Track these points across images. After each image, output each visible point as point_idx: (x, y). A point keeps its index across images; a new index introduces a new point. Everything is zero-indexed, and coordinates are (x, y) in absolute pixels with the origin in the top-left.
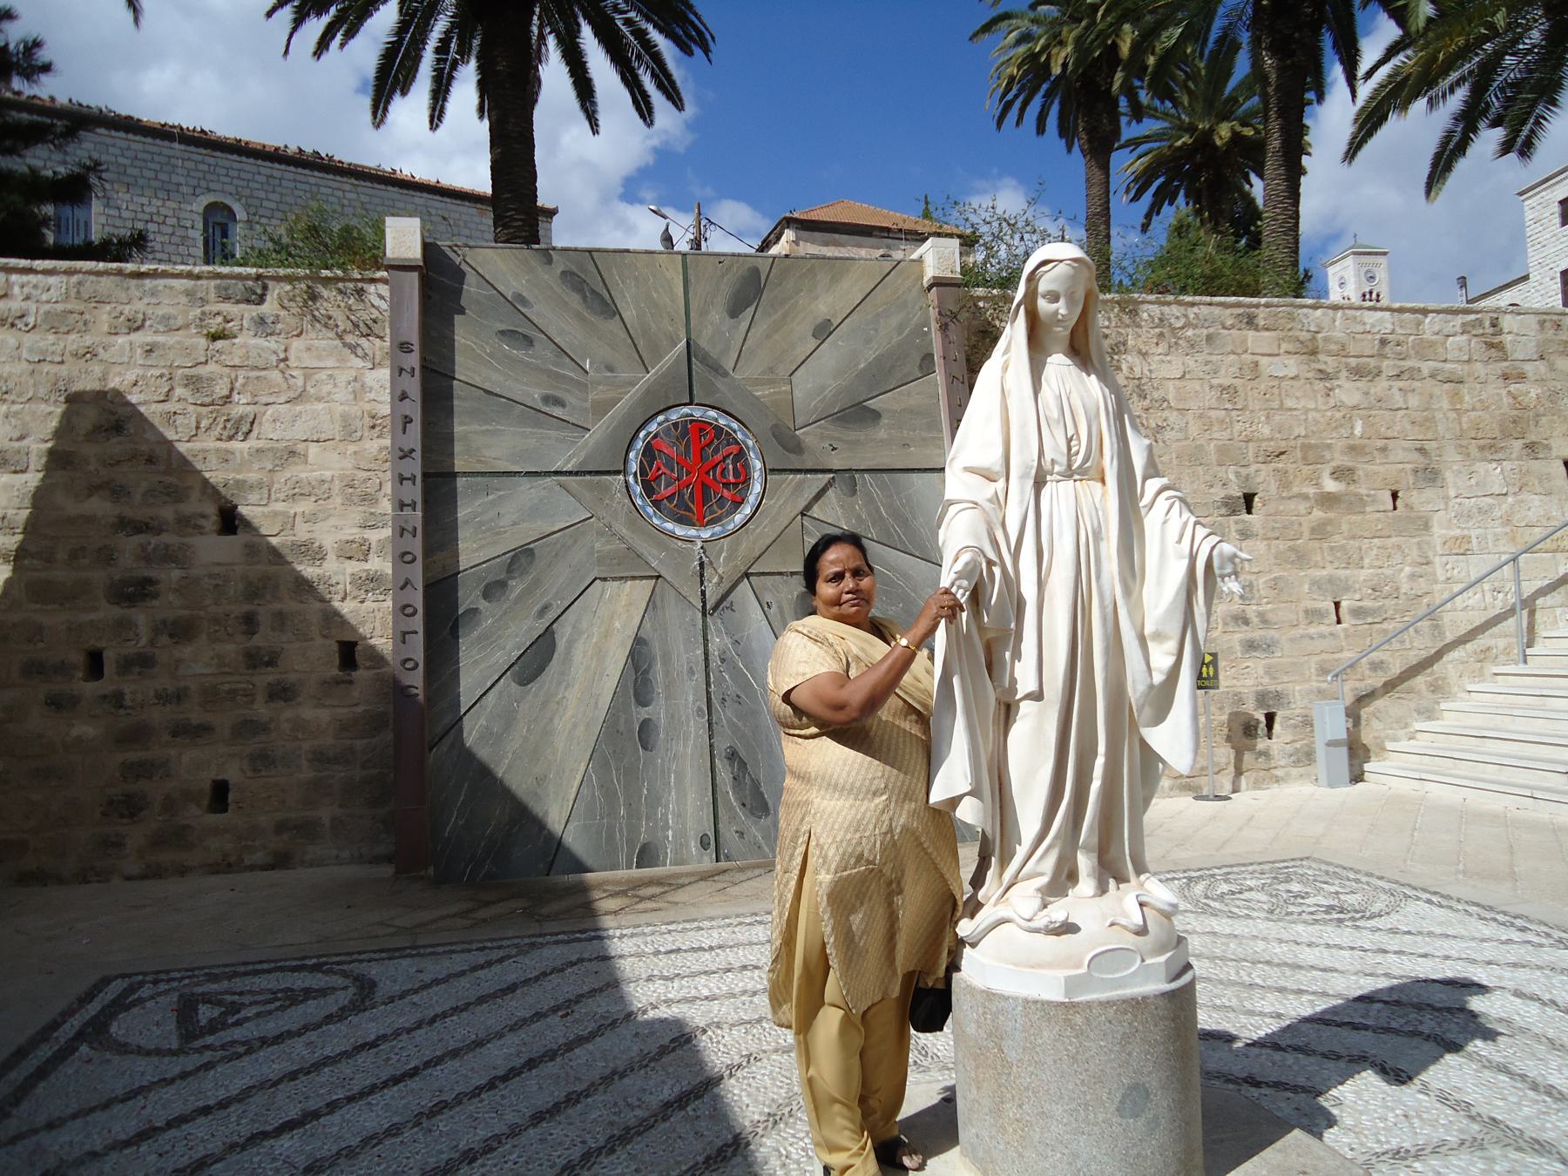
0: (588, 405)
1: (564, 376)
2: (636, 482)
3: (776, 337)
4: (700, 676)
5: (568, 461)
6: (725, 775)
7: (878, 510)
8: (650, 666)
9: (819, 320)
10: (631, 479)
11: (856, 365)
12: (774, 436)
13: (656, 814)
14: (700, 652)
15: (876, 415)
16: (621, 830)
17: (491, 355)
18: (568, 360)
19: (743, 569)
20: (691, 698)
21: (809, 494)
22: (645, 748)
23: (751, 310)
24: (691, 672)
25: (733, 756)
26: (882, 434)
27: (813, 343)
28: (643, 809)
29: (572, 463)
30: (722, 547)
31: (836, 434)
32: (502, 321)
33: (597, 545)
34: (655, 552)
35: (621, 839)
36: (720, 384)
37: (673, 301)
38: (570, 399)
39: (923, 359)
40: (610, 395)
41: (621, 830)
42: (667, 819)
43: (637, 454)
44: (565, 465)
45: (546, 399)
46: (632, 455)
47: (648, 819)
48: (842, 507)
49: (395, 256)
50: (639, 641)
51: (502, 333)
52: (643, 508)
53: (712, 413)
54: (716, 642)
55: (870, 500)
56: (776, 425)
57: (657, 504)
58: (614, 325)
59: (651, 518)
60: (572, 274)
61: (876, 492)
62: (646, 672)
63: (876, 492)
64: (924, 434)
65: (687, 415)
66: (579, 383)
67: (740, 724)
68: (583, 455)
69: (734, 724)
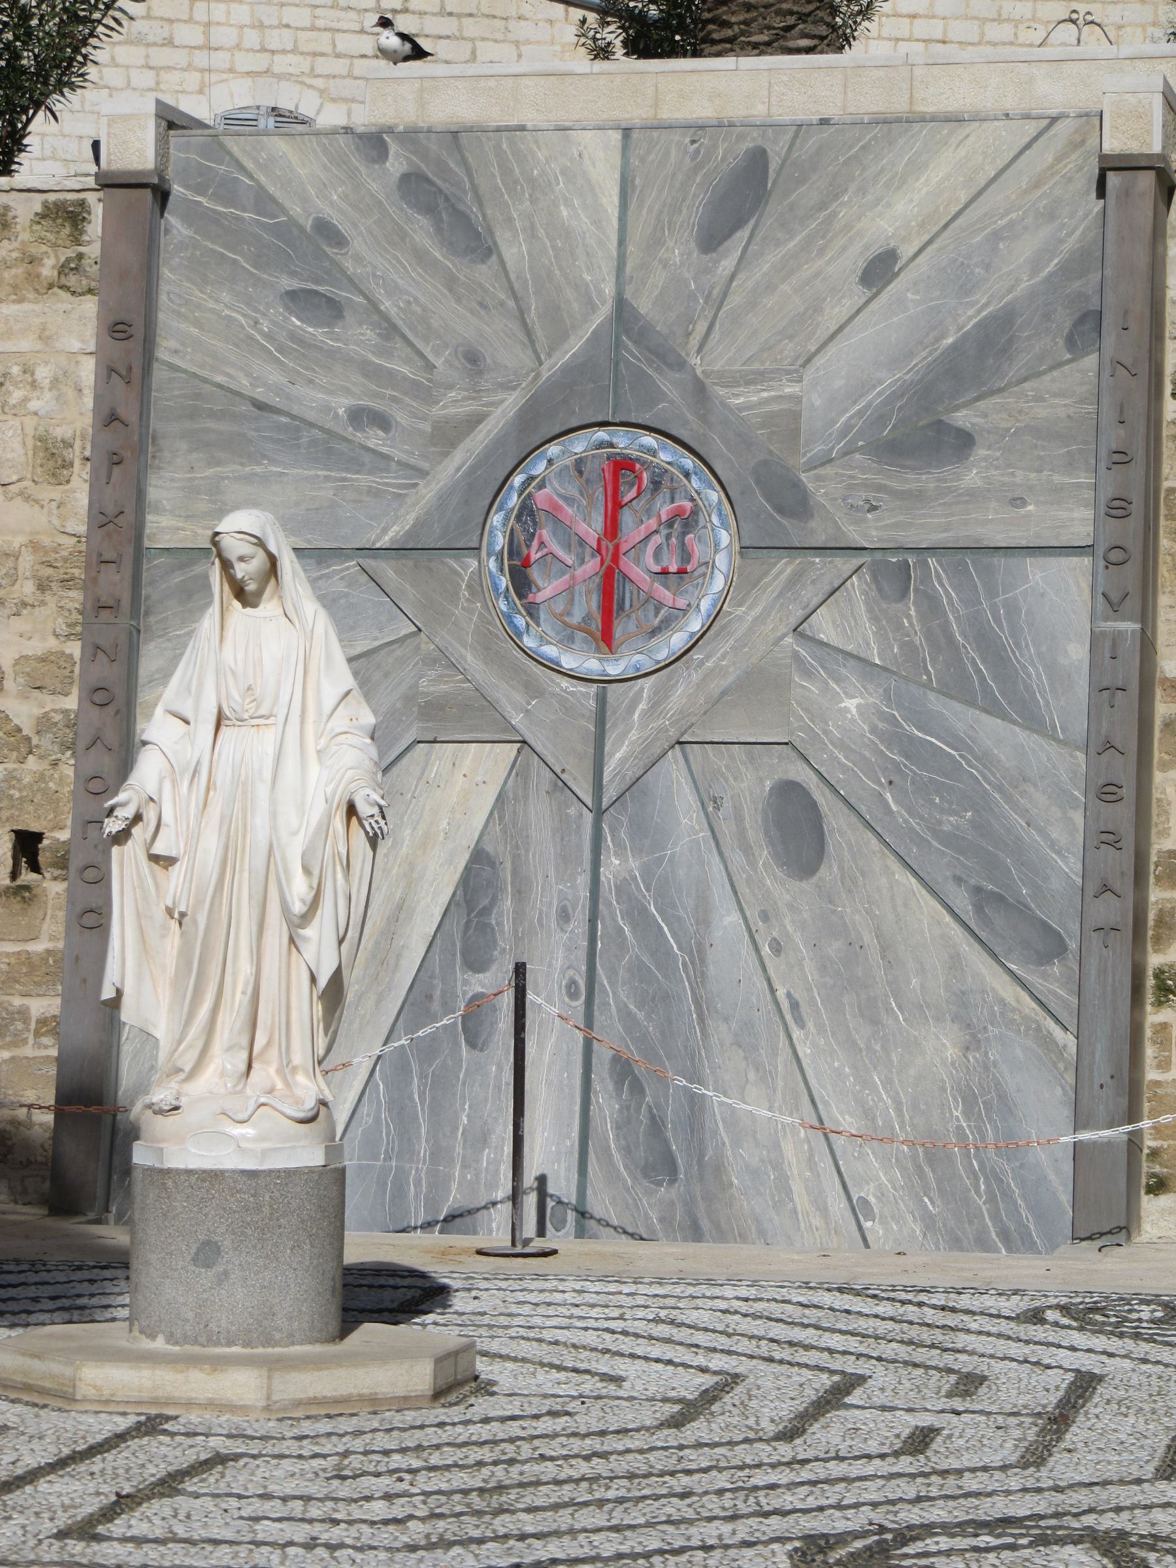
0: (427, 427)
1: (391, 373)
2: (502, 570)
3: (785, 288)
4: (578, 925)
5: (385, 530)
6: (606, 1104)
7: (946, 628)
8: (494, 901)
9: (871, 254)
10: (492, 564)
11: (937, 340)
12: (758, 482)
13: (478, 1161)
14: (583, 880)
15: (965, 441)
16: (418, 1183)
17: (269, 337)
18: (399, 343)
19: (673, 734)
20: (559, 964)
21: (810, 594)
22: (472, 1044)
23: (743, 234)
24: (564, 916)
25: (623, 1069)
26: (971, 477)
27: (860, 294)
28: (459, 1150)
29: (391, 534)
30: (642, 689)
31: (880, 480)
32: (293, 274)
33: (423, 682)
34: (518, 697)
35: (417, 1194)
36: (667, 384)
37: (597, 223)
38: (400, 417)
39: (1082, 320)
40: (471, 407)
41: (418, 1183)
42: (497, 1171)
43: (507, 518)
44: (378, 538)
45: (357, 416)
46: (496, 519)
47: (464, 1166)
48: (875, 619)
49: (114, 167)
50: (479, 856)
51: (292, 295)
52: (509, 618)
53: (649, 440)
54: (613, 866)
55: (932, 606)
56: (765, 463)
57: (532, 611)
58: (484, 272)
59: (519, 635)
60: (421, 177)
61: (945, 588)
62: (486, 911)
63: (945, 588)
64: (1057, 478)
65: (601, 445)
66: (416, 384)
67: (640, 1015)
68: (411, 519)
69: (629, 1013)
